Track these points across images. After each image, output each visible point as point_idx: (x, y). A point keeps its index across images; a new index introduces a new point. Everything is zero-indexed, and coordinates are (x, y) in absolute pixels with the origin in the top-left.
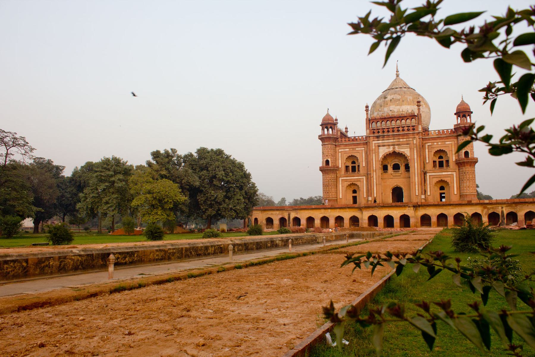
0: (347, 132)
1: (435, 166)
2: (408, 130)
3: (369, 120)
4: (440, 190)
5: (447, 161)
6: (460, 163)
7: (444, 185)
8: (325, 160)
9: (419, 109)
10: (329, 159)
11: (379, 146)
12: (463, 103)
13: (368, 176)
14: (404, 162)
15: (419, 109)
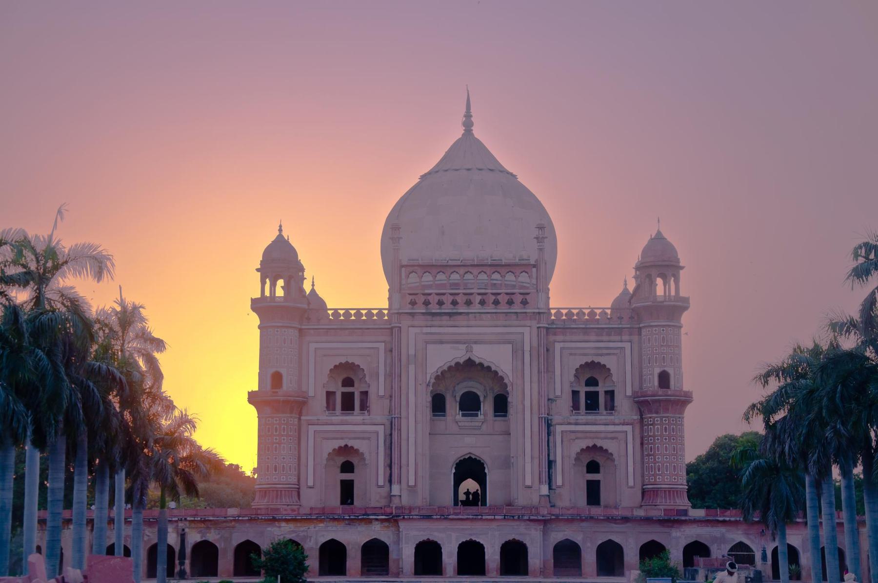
0: (303, 279)
1: (576, 406)
2: (510, 303)
3: (403, 266)
4: (588, 472)
5: (611, 394)
6: (646, 403)
7: (599, 459)
8: (272, 370)
9: (541, 250)
10: (283, 371)
11: (427, 343)
12: (659, 239)
13: (393, 428)
14: (492, 389)
15: (541, 250)
